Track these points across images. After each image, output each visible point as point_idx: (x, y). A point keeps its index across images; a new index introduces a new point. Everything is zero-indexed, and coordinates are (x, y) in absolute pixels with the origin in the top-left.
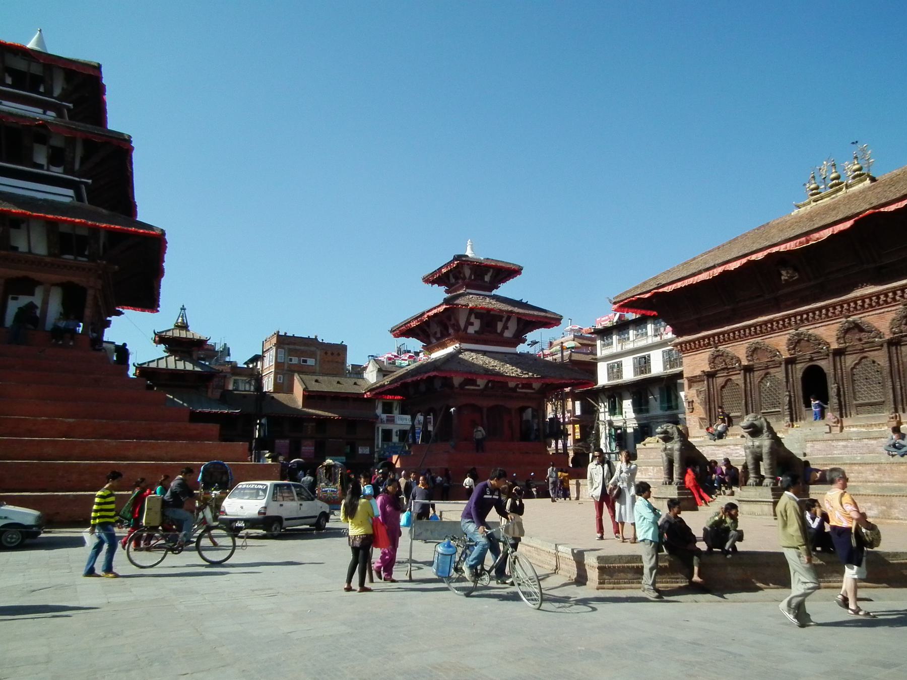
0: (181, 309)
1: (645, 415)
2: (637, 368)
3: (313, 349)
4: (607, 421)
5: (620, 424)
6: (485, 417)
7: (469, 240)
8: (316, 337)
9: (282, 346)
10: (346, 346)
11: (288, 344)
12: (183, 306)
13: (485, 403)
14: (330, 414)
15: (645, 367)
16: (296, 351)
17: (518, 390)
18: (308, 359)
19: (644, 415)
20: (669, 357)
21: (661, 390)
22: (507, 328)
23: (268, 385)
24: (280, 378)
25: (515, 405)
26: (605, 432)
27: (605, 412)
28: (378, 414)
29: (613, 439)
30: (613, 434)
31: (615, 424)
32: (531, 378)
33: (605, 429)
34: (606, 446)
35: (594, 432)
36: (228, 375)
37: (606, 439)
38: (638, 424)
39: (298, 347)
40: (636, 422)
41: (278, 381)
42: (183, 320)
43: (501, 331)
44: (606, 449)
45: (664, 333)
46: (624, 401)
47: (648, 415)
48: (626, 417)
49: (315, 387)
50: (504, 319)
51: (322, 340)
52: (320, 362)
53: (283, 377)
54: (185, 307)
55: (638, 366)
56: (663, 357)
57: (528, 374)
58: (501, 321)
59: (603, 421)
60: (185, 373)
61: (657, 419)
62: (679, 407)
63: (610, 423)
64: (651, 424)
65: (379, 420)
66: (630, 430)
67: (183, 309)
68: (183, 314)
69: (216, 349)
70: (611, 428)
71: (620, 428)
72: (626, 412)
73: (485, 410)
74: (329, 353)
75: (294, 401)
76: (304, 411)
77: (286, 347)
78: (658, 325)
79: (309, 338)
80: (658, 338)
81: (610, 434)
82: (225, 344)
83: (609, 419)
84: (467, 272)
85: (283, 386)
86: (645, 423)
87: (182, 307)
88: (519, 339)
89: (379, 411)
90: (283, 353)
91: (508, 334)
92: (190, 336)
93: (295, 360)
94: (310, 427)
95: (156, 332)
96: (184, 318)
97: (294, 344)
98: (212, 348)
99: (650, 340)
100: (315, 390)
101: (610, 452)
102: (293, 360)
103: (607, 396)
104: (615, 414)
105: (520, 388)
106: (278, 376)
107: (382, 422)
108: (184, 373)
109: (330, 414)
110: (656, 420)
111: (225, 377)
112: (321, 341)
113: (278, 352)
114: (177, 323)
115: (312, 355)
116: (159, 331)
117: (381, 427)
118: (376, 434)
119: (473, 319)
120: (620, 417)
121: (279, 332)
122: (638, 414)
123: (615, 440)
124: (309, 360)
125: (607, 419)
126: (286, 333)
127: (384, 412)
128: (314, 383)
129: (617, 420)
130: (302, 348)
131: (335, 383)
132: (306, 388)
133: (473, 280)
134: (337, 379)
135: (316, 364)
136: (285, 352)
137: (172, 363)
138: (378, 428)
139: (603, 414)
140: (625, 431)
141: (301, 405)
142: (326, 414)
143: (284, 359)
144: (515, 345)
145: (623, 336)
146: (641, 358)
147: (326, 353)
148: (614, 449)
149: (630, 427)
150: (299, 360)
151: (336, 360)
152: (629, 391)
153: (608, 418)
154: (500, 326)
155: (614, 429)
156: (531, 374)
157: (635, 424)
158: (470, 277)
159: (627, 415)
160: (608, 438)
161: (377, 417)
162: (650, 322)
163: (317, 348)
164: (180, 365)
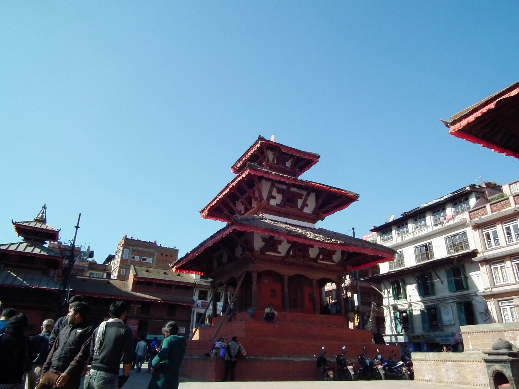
0: (43, 208)
1: (432, 298)
2: (419, 255)
3: (152, 250)
4: (392, 305)
5: (406, 307)
6: (286, 286)
7: (273, 136)
8: (155, 242)
9: (128, 247)
10: (178, 250)
11: (133, 246)
12: (45, 205)
13: (287, 272)
14: (154, 298)
15: (427, 253)
16: (139, 251)
17: (319, 261)
18: (147, 258)
19: (430, 297)
20: (453, 243)
21: (448, 272)
22: (307, 205)
23: (114, 275)
24: (123, 271)
25: (317, 276)
26: (390, 315)
27: (388, 297)
28: (195, 300)
29: (398, 321)
30: (398, 316)
31: (400, 308)
32: (335, 244)
33: (390, 313)
34: (392, 328)
35: (370, 320)
36: (86, 269)
37: (391, 321)
38: (424, 306)
39: (140, 249)
40: (423, 305)
41: (121, 273)
42: (42, 216)
43: (301, 207)
44: (392, 331)
45: (445, 221)
46: (407, 286)
47: (434, 297)
48: (411, 300)
49: (144, 274)
50: (303, 197)
51: (160, 245)
52: (156, 261)
53: (126, 271)
54: (46, 206)
55: (420, 254)
56: (446, 243)
57: (331, 241)
58: (301, 198)
59: (388, 306)
60: (31, 255)
61: (446, 300)
62: (470, 288)
63: (395, 308)
64: (440, 306)
65: (195, 305)
66: (416, 313)
67: (45, 207)
68: (44, 211)
69: (81, 251)
70: (396, 311)
71: (405, 311)
72: (410, 296)
73: (286, 279)
74: (164, 255)
75: (127, 286)
76: (133, 295)
77: (131, 248)
78: (437, 216)
79: (149, 242)
80: (439, 227)
81: (395, 318)
82: (89, 247)
83: (393, 303)
84: (270, 155)
85: (123, 277)
86: (431, 306)
87: (43, 206)
88: (318, 215)
89: (196, 297)
90: (128, 252)
91: (307, 210)
92: (44, 227)
93: (137, 258)
94: (136, 308)
95: (14, 222)
96: (44, 215)
97: (138, 246)
98: (78, 249)
99: (431, 229)
100: (143, 277)
101: (396, 334)
102: (135, 259)
103: (390, 282)
104: (398, 299)
105: (320, 260)
106: (122, 269)
107: (198, 306)
108: (31, 257)
109: (154, 298)
110: (445, 302)
111: (83, 270)
112: (159, 246)
113: (124, 251)
114: (37, 218)
115: (151, 255)
116: (17, 221)
117: (196, 311)
118: (192, 317)
119: (274, 193)
120: (404, 301)
121: (126, 236)
122: (423, 297)
123: (400, 323)
124: (148, 259)
125: (391, 304)
126: (132, 238)
127: (200, 298)
128: (144, 272)
129: (402, 304)
130: (144, 249)
131: (162, 274)
132: (137, 274)
133: (275, 164)
134: (164, 271)
135: (153, 262)
136: (129, 252)
137: (26, 248)
138: (194, 311)
139: (387, 299)
140: (411, 313)
141: (131, 290)
142: (151, 297)
143: (128, 257)
144: (314, 221)
145: (401, 230)
146: (422, 246)
147: (162, 255)
148: (400, 332)
149: (416, 310)
150: (140, 258)
151: (169, 260)
152: (413, 276)
153: (392, 302)
154: (300, 202)
155: (400, 312)
156: (334, 240)
157: (422, 306)
158: (273, 160)
159: (411, 298)
160: (394, 321)
161: (193, 302)
162: (429, 213)
163: (155, 250)
164: (29, 250)
